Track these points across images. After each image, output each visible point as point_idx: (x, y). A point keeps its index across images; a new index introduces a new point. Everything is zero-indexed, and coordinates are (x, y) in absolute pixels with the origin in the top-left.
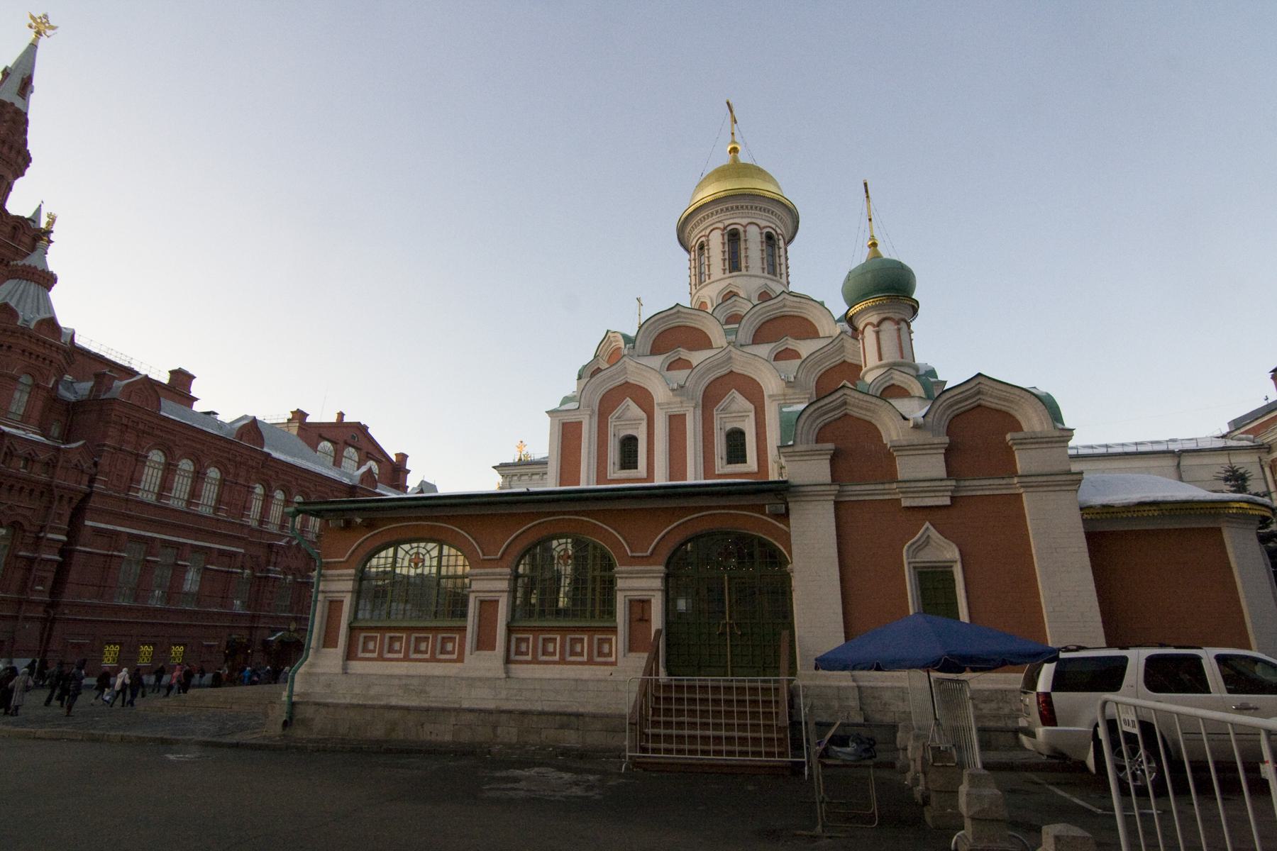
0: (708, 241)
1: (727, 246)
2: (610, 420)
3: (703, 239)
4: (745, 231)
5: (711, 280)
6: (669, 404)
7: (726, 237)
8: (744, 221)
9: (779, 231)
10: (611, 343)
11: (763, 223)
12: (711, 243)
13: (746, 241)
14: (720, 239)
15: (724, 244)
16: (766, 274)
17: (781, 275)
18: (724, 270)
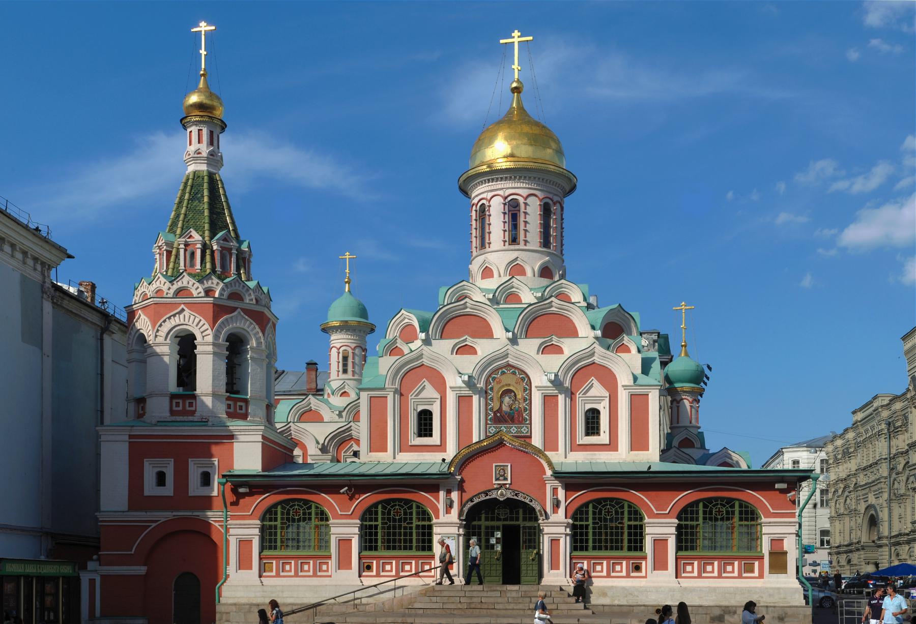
0: (490, 206)
2: (410, 398)
6: (460, 387)
7: (507, 207)
8: (525, 193)
18: (505, 241)
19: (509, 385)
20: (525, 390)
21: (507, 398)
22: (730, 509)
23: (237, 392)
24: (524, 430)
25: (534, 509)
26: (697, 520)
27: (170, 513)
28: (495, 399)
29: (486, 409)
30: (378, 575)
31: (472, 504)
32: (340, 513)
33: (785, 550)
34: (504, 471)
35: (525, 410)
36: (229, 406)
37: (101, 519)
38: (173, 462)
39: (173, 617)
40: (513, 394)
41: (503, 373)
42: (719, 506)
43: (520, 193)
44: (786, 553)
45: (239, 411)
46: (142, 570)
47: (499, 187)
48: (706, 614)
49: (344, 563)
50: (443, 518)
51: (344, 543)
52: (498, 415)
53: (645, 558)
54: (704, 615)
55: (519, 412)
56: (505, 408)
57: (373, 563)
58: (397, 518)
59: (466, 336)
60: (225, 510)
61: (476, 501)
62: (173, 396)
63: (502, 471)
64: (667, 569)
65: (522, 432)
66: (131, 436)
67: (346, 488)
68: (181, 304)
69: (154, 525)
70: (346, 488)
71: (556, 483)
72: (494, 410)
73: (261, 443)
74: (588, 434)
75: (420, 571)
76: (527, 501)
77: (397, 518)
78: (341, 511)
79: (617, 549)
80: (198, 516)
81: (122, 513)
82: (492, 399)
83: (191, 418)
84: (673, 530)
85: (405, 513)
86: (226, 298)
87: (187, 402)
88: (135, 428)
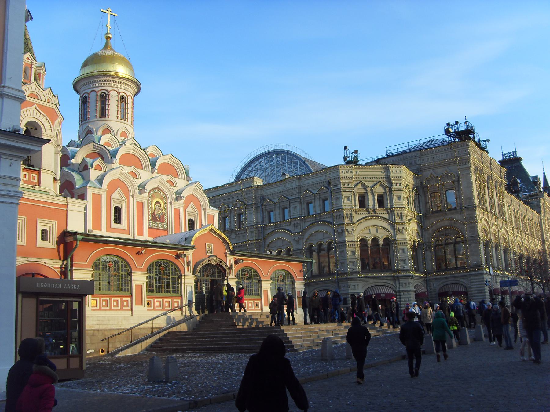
0: (108, 95)
8: (128, 93)
15: (118, 101)
18: (118, 117)
20: (164, 203)
21: (157, 206)
29: (148, 211)
30: (154, 309)
32: (137, 267)
43: (127, 94)
50: (186, 273)
52: (154, 216)
55: (163, 215)
56: (156, 213)
76: (224, 266)
80: (45, 263)
85: (166, 270)
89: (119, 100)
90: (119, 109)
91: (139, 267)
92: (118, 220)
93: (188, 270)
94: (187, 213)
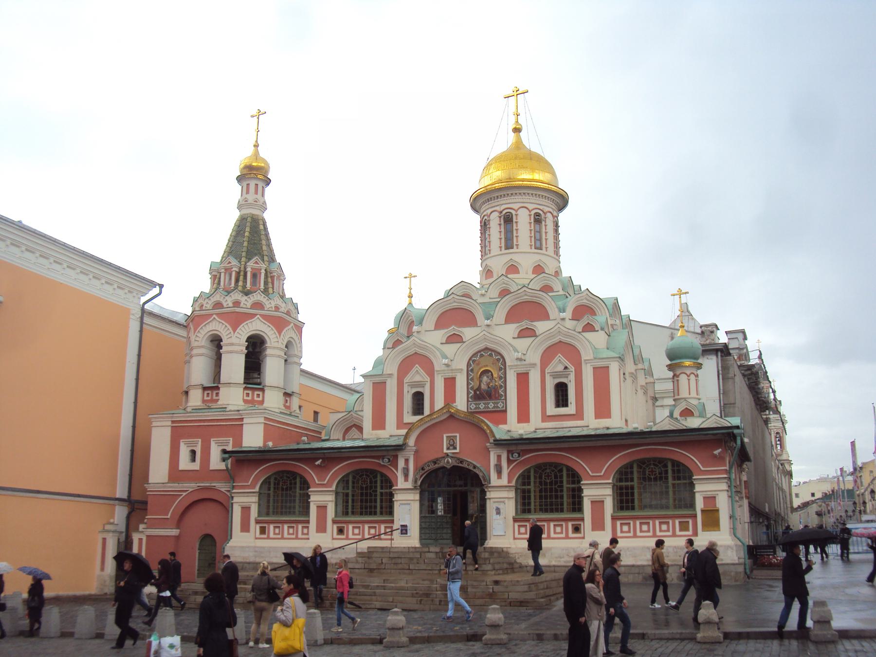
0: (489, 220)
1: (502, 226)
2: (405, 381)
3: (486, 217)
4: (516, 215)
5: (491, 255)
6: (444, 370)
8: (515, 206)
9: (546, 209)
10: (409, 316)
11: (531, 207)
12: (491, 222)
13: (516, 222)
14: (497, 221)
15: (500, 225)
16: (534, 250)
17: (546, 248)
18: (501, 247)
19: (487, 366)
20: (500, 369)
22: (663, 469)
23: (259, 384)
24: (500, 405)
25: (477, 476)
26: (632, 480)
27: (194, 485)
28: (475, 380)
30: (347, 538)
31: (423, 472)
32: (317, 482)
33: (717, 506)
34: (454, 441)
35: (501, 386)
36: (248, 395)
37: (148, 489)
38: (200, 443)
39: (196, 572)
40: (490, 373)
41: (482, 356)
42: (652, 466)
44: (718, 511)
45: (256, 398)
46: (175, 532)
47: (496, 204)
48: (639, 573)
49: (321, 528)
50: (401, 483)
51: (322, 509)
52: (478, 393)
53: (582, 519)
54: (636, 575)
55: (496, 389)
56: (484, 387)
57: (344, 527)
58: (364, 486)
59: (453, 327)
60: (232, 482)
61: (427, 469)
62: (205, 389)
63: (451, 441)
64: (603, 529)
65: (498, 407)
66: (173, 422)
67: (321, 460)
68: (212, 315)
69: (184, 494)
70: (321, 460)
71: (499, 451)
72: (476, 387)
73: (262, 425)
74: (558, 405)
75: (383, 531)
76: (471, 468)
77: (364, 486)
78: (319, 481)
79: (557, 511)
80: (215, 486)
81: (162, 485)
82: (472, 379)
83: (214, 405)
84: (609, 491)
85: (371, 482)
86: (249, 307)
87: (215, 392)
88: (175, 415)
89: (502, 222)
90: (503, 236)
91: (319, 483)
92: (418, 408)
93: (406, 479)
94: (548, 377)
